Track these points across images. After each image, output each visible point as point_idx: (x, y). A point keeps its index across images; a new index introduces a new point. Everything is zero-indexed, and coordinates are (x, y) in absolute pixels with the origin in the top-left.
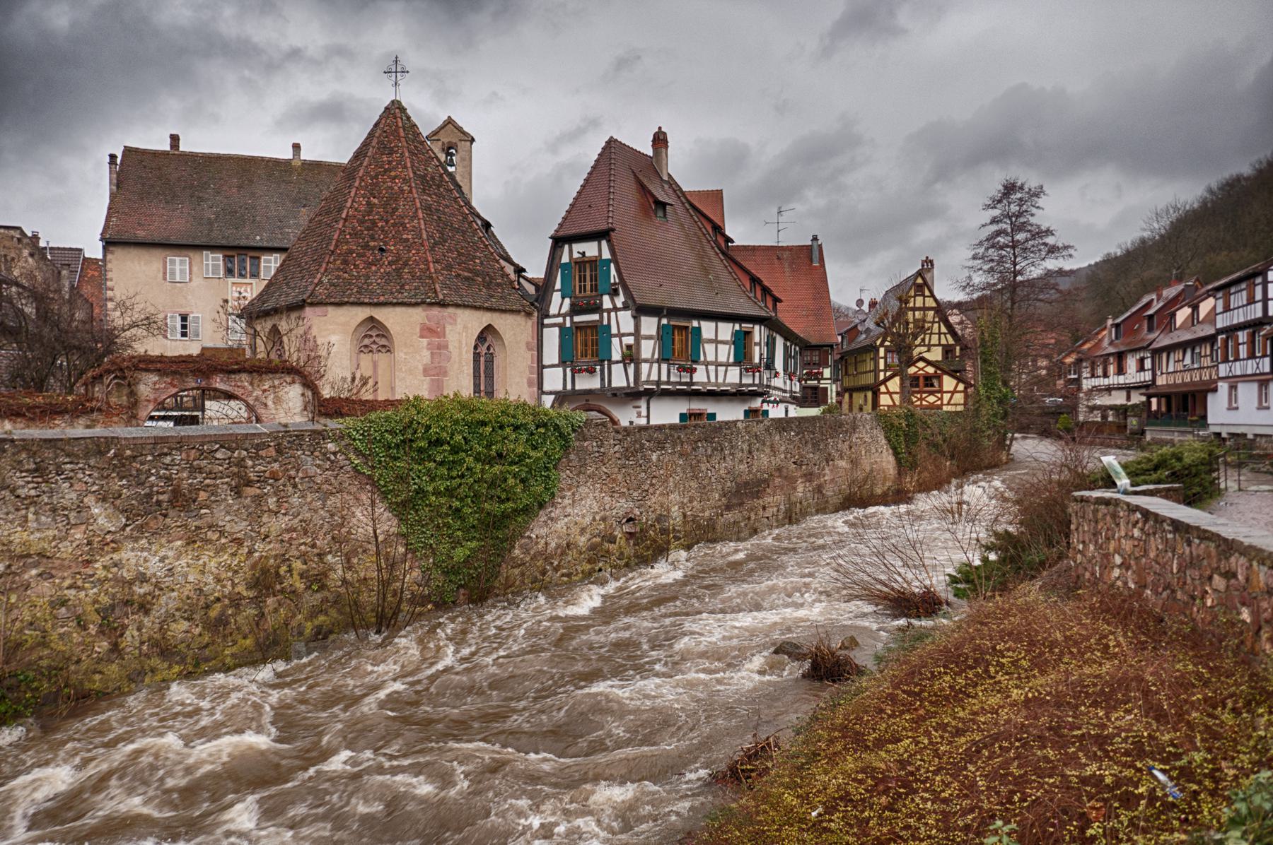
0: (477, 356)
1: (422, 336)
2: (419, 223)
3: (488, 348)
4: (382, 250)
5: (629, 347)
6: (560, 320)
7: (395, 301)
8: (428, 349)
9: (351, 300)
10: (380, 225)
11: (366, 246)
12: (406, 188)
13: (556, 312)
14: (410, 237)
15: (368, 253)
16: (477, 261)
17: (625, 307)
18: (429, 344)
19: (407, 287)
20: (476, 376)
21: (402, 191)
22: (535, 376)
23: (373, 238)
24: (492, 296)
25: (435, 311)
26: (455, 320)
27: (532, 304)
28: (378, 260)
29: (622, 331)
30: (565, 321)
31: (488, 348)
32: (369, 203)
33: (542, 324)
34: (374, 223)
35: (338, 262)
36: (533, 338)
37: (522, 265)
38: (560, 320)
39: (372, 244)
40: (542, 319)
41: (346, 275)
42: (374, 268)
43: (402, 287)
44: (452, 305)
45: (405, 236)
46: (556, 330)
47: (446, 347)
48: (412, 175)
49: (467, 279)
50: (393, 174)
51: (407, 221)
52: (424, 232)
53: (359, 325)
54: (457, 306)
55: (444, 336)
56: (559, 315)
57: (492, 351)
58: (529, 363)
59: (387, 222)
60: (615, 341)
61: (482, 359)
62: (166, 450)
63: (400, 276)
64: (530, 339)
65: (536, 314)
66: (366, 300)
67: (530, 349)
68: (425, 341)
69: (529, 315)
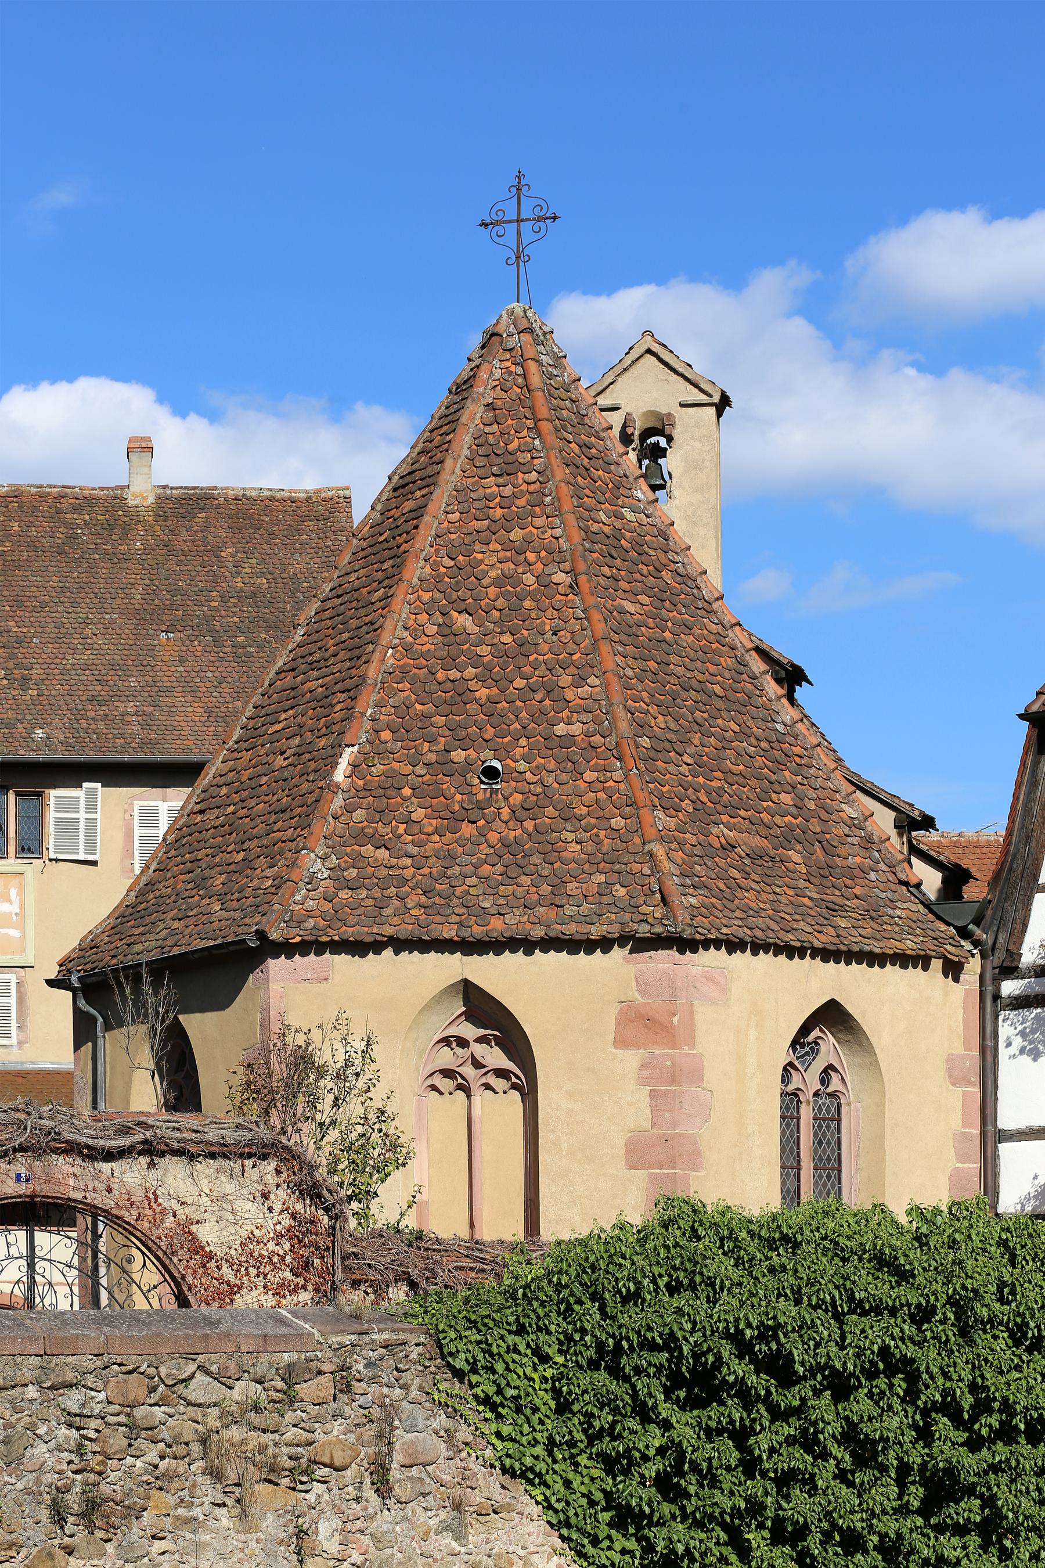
0: (791, 1100)
1: (621, 1042)
2: (606, 686)
3: (825, 1080)
4: (491, 773)
7: (538, 932)
8: (642, 1082)
9: (406, 931)
10: (483, 693)
11: (444, 766)
12: (559, 577)
14: (576, 729)
15: (447, 786)
16: (786, 798)
18: (643, 1066)
19: (572, 887)
20: (790, 1166)
21: (545, 583)
22: (974, 1166)
24: (833, 909)
25: (664, 959)
26: (724, 990)
27: (964, 933)
28: (480, 806)
31: (825, 1080)
32: (447, 631)
33: (997, 997)
34: (462, 695)
35: (359, 814)
36: (967, 1047)
37: (923, 803)
39: (459, 755)
40: (997, 981)
41: (382, 854)
42: (467, 830)
43: (558, 884)
44: (717, 944)
45: (561, 729)
47: (697, 1075)
48: (577, 536)
49: (757, 856)
50: (517, 534)
52: (621, 713)
53: (427, 1008)
54: (734, 946)
55: (693, 1046)
57: (835, 1084)
58: (956, 1121)
59: (503, 682)
61: (806, 1113)
62: (70, 1376)
63: (551, 851)
64: (959, 1049)
65: (974, 966)
66: (449, 933)
67: (955, 1080)
68: (631, 1059)
69: (953, 969)
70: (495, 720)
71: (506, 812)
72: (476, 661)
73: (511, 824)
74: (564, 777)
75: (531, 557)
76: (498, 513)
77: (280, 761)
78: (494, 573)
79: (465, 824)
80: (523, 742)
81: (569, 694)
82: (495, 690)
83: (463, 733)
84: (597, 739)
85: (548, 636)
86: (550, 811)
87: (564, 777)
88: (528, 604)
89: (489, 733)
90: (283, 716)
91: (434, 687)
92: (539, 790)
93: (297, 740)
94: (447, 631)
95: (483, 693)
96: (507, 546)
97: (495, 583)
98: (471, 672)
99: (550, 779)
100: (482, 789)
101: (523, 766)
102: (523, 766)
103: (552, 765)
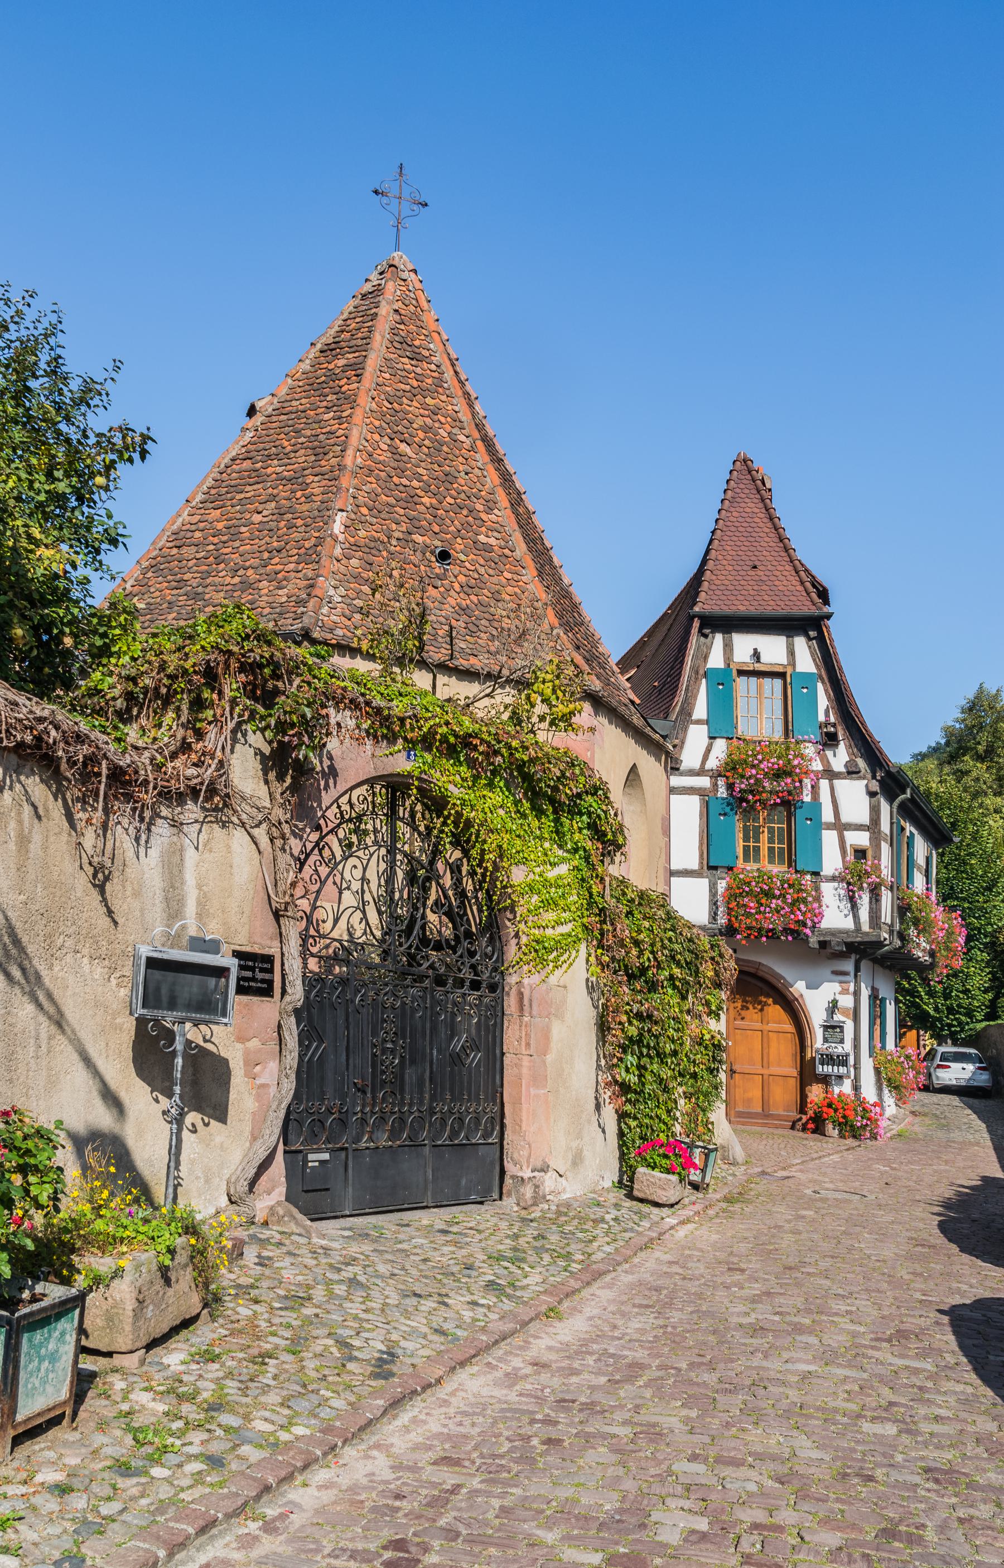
5: (860, 853)
6: (705, 782)
12: (462, 438)
13: (696, 765)
14: (492, 541)
17: (852, 772)
23: (415, 525)
29: (845, 818)
30: (715, 785)
32: (394, 451)
34: (411, 500)
38: (705, 782)
45: (482, 538)
46: (694, 802)
51: (479, 507)
56: (701, 772)
60: (829, 839)
70: (437, 520)
71: (457, 586)
72: (419, 477)
73: (462, 595)
74: (491, 572)
75: (443, 419)
76: (415, 384)
77: (257, 518)
78: (420, 421)
79: (430, 588)
80: (459, 540)
81: (484, 516)
82: (434, 501)
83: (417, 524)
84: (506, 551)
85: (463, 474)
86: (485, 591)
87: (491, 572)
88: (445, 448)
89: (436, 529)
90: (248, 488)
91: (393, 487)
92: (476, 576)
93: (273, 504)
94: (394, 451)
95: (426, 500)
96: (424, 406)
97: (421, 428)
98: (415, 483)
99: (482, 570)
100: (438, 568)
101: (463, 557)
102: (463, 557)
103: (482, 562)
